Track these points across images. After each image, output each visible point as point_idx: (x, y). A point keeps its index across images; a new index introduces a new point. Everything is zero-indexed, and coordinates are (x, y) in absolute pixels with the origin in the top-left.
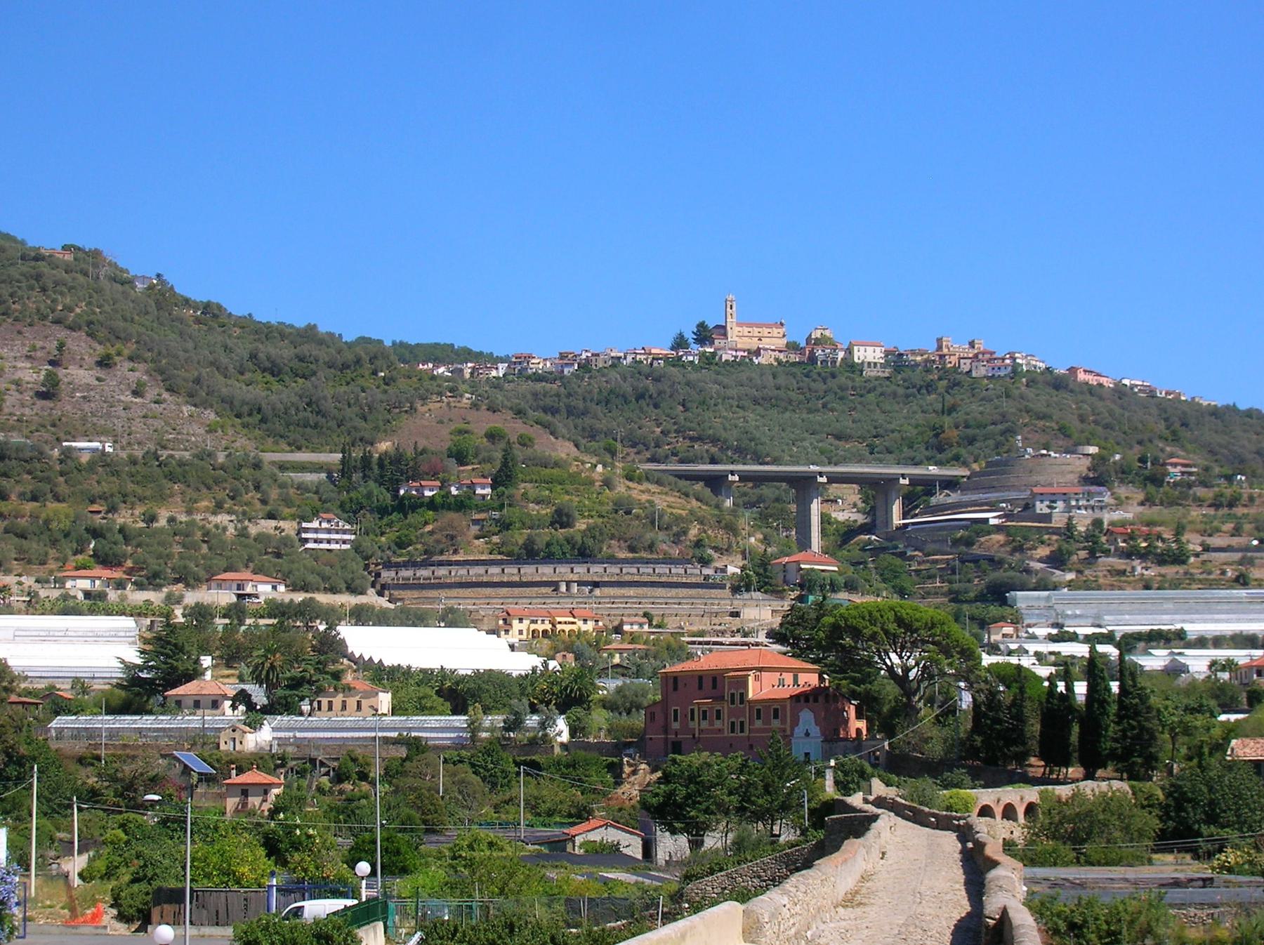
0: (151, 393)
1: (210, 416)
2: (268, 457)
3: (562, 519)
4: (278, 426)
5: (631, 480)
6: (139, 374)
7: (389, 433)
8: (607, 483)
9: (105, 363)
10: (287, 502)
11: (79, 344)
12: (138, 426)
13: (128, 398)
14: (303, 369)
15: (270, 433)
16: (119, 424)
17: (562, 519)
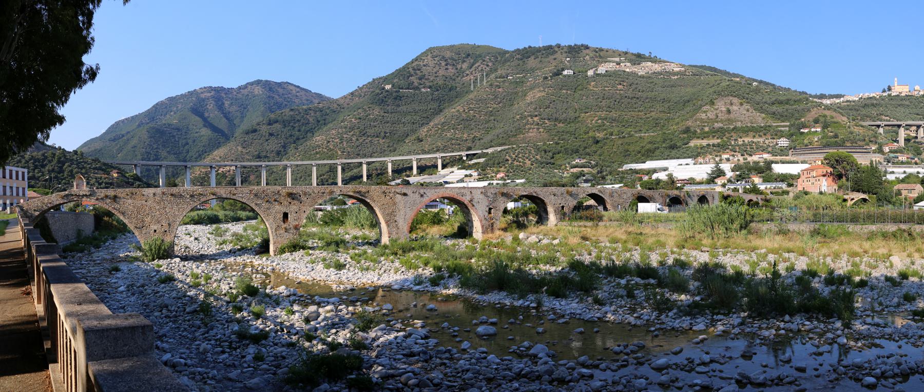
0: (751, 111)
1: (763, 115)
2: (774, 124)
3: (836, 136)
4: (779, 117)
5: (856, 126)
6: (748, 107)
7: (803, 117)
8: (849, 127)
9: (741, 104)
10: (776, 135)
11: (735, 100)
12: (747, 119)
13: (745, 112)
14: (787, 102)
15: (776, 118)
16: (742, 119)
17: (836, 136)
